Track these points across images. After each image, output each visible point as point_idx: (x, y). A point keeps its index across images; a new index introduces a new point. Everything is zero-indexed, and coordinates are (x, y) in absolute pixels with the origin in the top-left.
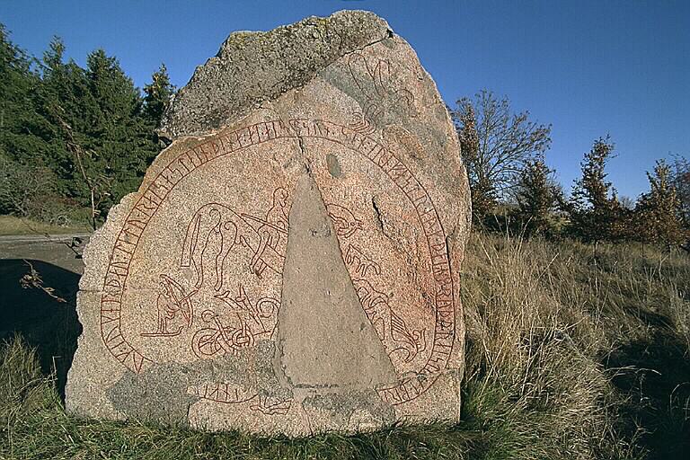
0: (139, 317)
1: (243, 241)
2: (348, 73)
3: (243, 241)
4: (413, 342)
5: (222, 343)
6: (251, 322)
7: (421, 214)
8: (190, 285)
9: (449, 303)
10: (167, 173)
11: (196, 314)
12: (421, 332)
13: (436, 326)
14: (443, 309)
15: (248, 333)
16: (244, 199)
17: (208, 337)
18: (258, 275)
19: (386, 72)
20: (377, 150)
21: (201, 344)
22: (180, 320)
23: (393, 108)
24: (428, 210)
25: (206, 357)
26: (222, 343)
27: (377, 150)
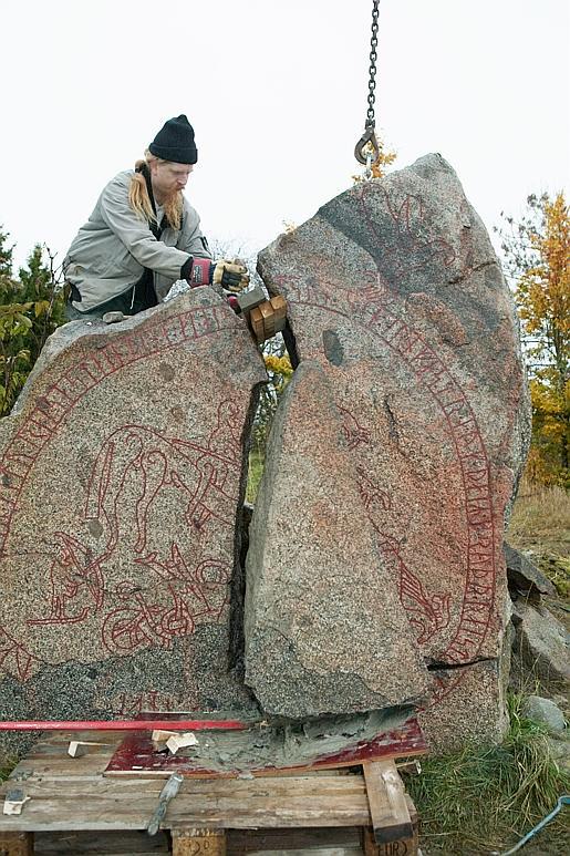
0: (25, 595)
1: (175, 479)
2: (360, 212)
3: (175, 479)
4: (431, 613)
5: (147, 630)
6: (187, 597)
8: (98, 545)
9: (486, 558)
10: (65, 384)
11: (110, 588)
12: (443, 599)
13: (467, 592)
15: (185, 614)
16: (177, 415)
17: (126, 622)
18: (198, 526)
19: (416, 213)
20: (395, 328)
21: (116, 633)
22: (86, 598)
24: (465, 420)
25: (121, 653)
26: (147, 630)
27: (395, 328)
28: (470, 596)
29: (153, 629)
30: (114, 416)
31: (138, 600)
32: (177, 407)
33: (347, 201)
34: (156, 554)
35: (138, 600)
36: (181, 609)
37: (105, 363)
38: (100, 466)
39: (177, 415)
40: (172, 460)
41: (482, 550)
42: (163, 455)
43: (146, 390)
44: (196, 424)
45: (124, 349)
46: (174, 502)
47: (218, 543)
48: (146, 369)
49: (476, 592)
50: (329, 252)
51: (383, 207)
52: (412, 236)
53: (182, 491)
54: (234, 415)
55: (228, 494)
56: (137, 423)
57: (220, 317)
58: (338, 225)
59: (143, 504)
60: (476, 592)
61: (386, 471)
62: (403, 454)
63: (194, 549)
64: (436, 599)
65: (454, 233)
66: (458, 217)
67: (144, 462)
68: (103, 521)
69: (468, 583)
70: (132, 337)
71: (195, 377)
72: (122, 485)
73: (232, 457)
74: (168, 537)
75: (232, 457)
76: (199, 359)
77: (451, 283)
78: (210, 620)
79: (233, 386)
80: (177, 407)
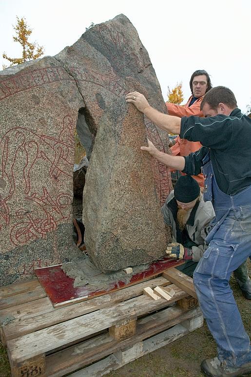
1: (43, 155)
6: (53, 213)
7: (150, 132)
9: (166, 184)
14: (164, 188)
15: (52, 221)
17: (22, 229)
18: (56, 178)
23: (128, 66)
27: (123, 92)
28: (162, 200)
29: (37, 231)
30: (8, 122)
31: (28, 217)
32: (42, 118)
33: (93, 32)
35: (28, 217)
36: (50, 219)
39: (42, 122)
40: (41, 145)
41: (164, 182)
42: (36, 143)
43: (25, 109)
44: (52, 128)
45: (11, 85)
47: (66, 186)
48: (23, 97)
49: (164, 198)
50: (90, 57)
51: (108, 36)
52: (122, 51)
53: (47, 161)
54: (71, 123)
55: (69, 162)
56: (21, 126)
57: (61, 73)
58: (91, 43)
59: (27, 169)
60: (164, 198)
63: (55, 189)
65: (137, 51)
66: (137, 44)
67: (27, 147)
68: (6, 179)
69: (161, 195)
70: (15, 79)
71: (51, 103)
72: (15, 159)
73: (71, 144)
74: (41, 185)
75: (71, 144)
76: (52, 94)
77: (139, 73)
78: (64, 222)
79: (70, 108)
80: (42, 118)
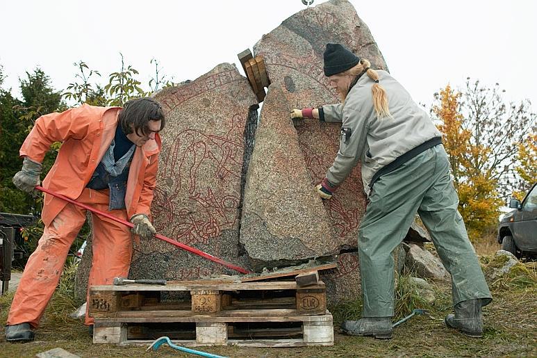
1: (210, 155)
12: (354, 212)
15: (215, 225)
16: (211, 123)
18: (222, 179)
26: (195, 234)
29: (198, 234)
32: (212, 119)
34: (200, 194)
37: (176, 100)
38: (173, 150)
39: (211, 123)
43: (196, 112)
44: (221, 128)
46: (210, 167)
47: (232, 188)
48: (196, 102)
54: (240, 121)
59: (194, 168)
61: (320, 145)
62: (329, 136)
64: (350, 212)
68: (173, 178)
71: (220, 104)
74: (206, 185)
76: (223, 95)
78: (228, 228)
